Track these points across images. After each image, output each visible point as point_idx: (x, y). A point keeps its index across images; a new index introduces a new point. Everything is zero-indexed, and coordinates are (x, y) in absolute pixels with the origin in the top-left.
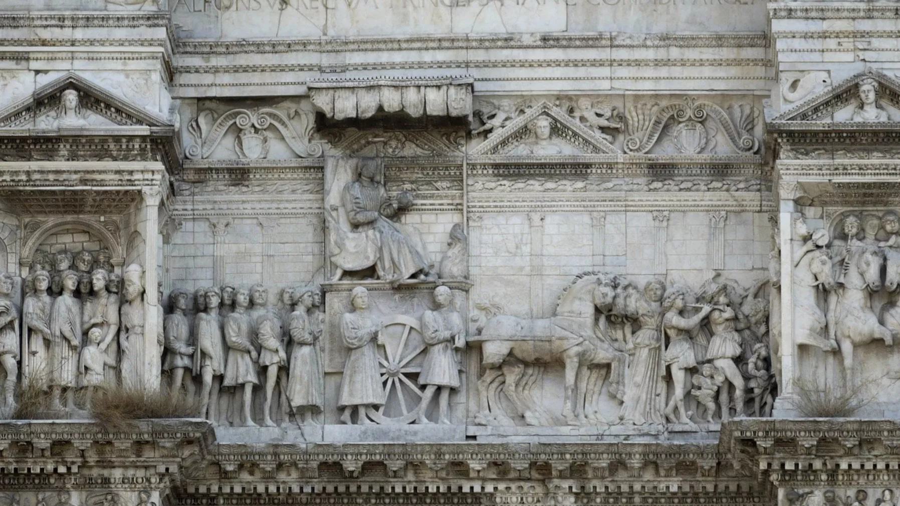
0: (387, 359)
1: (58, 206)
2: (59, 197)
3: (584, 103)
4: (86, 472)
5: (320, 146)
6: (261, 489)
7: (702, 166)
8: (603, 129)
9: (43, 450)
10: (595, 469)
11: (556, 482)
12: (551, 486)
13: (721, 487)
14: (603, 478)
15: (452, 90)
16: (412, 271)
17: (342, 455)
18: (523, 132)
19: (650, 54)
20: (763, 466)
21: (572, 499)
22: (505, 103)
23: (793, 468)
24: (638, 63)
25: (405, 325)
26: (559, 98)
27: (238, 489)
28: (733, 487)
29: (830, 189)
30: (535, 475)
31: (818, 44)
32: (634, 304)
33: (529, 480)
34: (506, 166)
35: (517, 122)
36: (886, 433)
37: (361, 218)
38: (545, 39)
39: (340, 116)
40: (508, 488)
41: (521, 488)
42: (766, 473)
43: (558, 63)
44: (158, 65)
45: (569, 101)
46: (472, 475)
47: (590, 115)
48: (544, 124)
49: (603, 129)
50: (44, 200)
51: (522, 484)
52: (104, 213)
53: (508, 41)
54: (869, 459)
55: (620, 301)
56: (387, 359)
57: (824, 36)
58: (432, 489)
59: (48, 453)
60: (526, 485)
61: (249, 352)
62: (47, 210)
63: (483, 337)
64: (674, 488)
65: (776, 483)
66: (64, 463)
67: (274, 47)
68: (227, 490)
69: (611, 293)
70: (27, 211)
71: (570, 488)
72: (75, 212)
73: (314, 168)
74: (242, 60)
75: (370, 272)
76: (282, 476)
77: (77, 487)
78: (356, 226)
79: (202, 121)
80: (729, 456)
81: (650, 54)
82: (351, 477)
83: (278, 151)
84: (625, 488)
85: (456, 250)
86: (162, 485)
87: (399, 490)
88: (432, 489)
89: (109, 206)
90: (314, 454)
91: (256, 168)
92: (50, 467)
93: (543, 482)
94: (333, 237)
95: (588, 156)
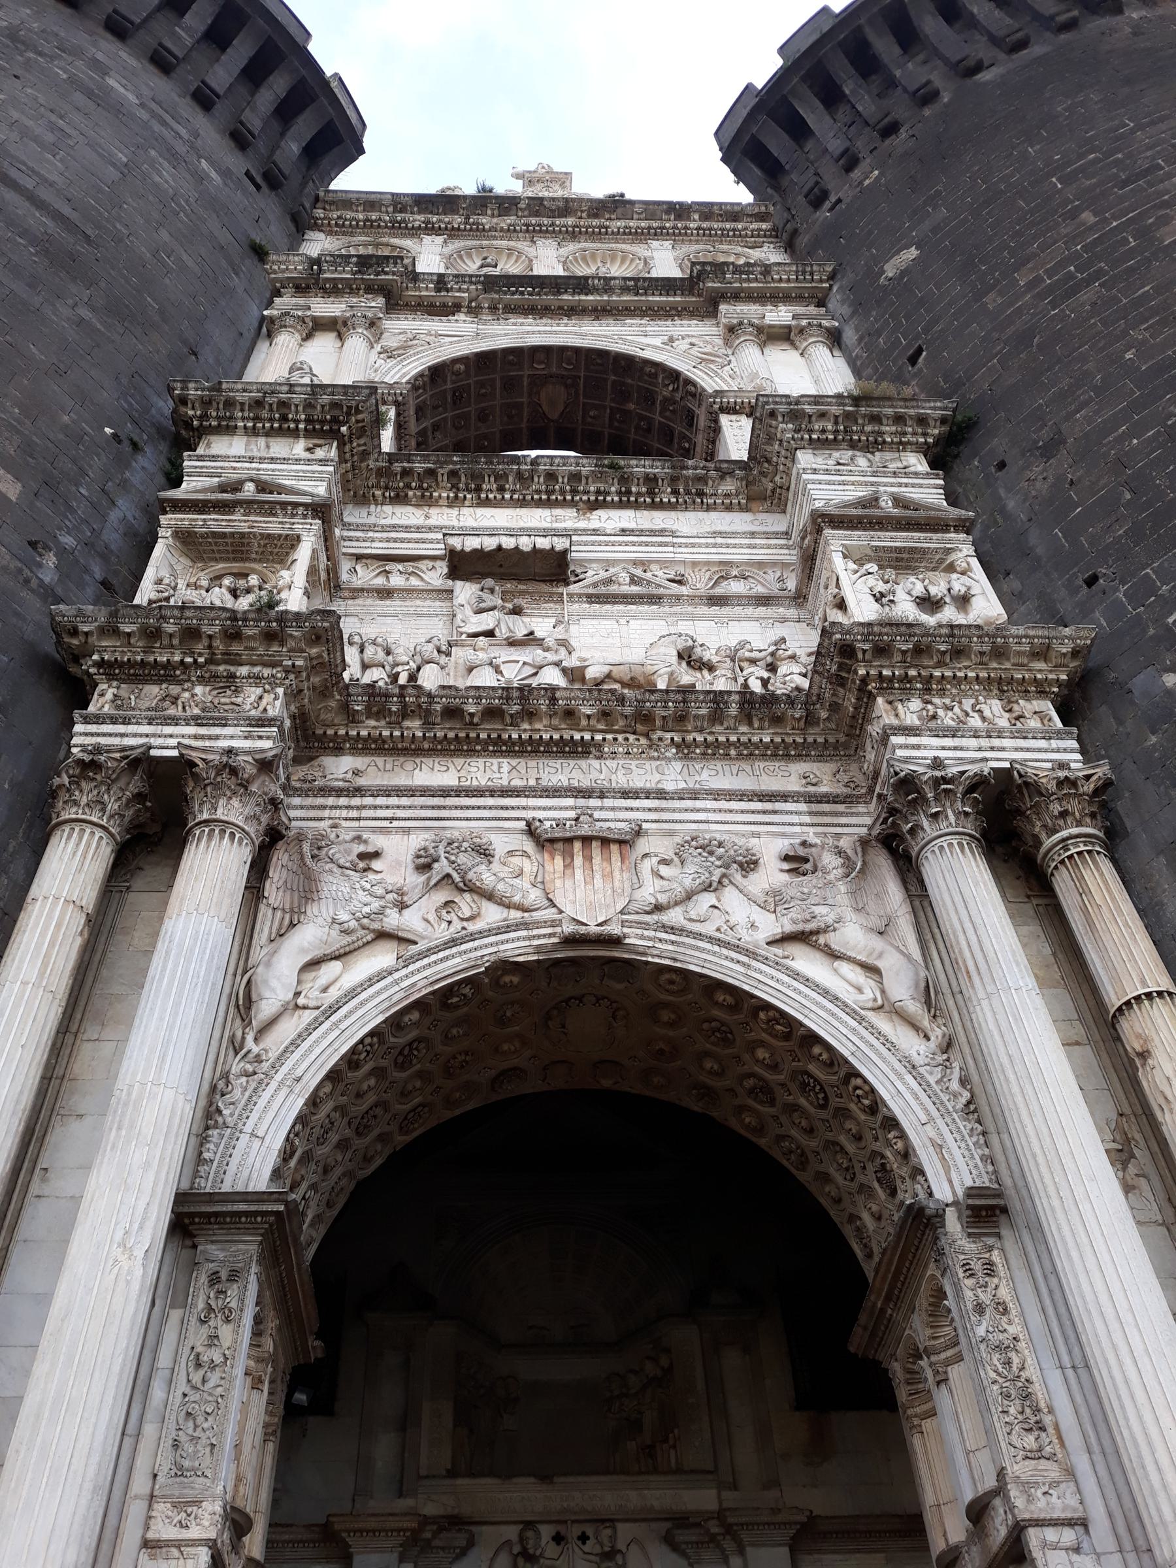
0: (503, 676)
1: (228, 552)
2: (229, 541)
3: (654, 567)
4: (213, 667)
5: (450, 582)
6: (386, 733)
7: (749, 597)
8: (670, 580)
9: (171, 636)
10: (696, 717)
11: (659, 733)
12: (655, 736)
13: (810, 739)
14: (701, 731)
15: (555, 538)
16: (526, 632)
17: (464, 697)
18: (609, 581)
19: (703, 541)
20: (862, 672)
21: (674, 751)
22: (594, 565)
23: (890, 673)
24: (693, 545)
25: (518, 662)
26: (635, 563)
27: (364, 733)
28: (820, 740)
29: (869, 552)
30: (639, 727)
31: (841, 487)
32: (708, 655)
33: (634, 733)
34: (598, 596)
35: (603, 575)
36: (975, 639)
37: (483, 605)
38: (623, 530)
39: (468, 549)
40: (615, 739)
41: (627, 739)
42: (865, 680)
43: (634, 544)
44: (325, 484)
45: (644, 564)
46: (584, 722)
47: (660, 573)
48: (624, 577)
49: (670, 580)
50: (216, 543)
51: (628, 735)
52: (267, 561)
53: (595, 532)
54: (960, 669)
55: (698, 650)
56: (503, 676)
57: (844, 483)
58: (546, 736)
59: (176, 641)
60: (632, 737)
61: (383, 667)
62: (218, 556)
63: (586, 664)
64: (767, 739)
65: (875, 691)
66: (192, 654)
67: (419, 529)
68: (353, 733)
69: (690, 643)
70: (202, 559)
71: (672, 739)
72: (243, 560)
73: (446, 591)
74: (393, 535)
75: (490, 634)
76: (407, 723)
77: (202, 680)
78: (479, 612)
79: (358, 568)
80: (818, 706)
81: (703, 541)
82: (471, 723)
83: (414, 582)
84: (722, 739)
85: (560, 628)
86: (287, 682)
87: (515, 736)
88: (546, 736)
89: (271, 553)
90: (437, 696)
91: (400, 590)
92: (177, 658)
93: (647, 736)
94: (459, 617)
95: (662, 591)
